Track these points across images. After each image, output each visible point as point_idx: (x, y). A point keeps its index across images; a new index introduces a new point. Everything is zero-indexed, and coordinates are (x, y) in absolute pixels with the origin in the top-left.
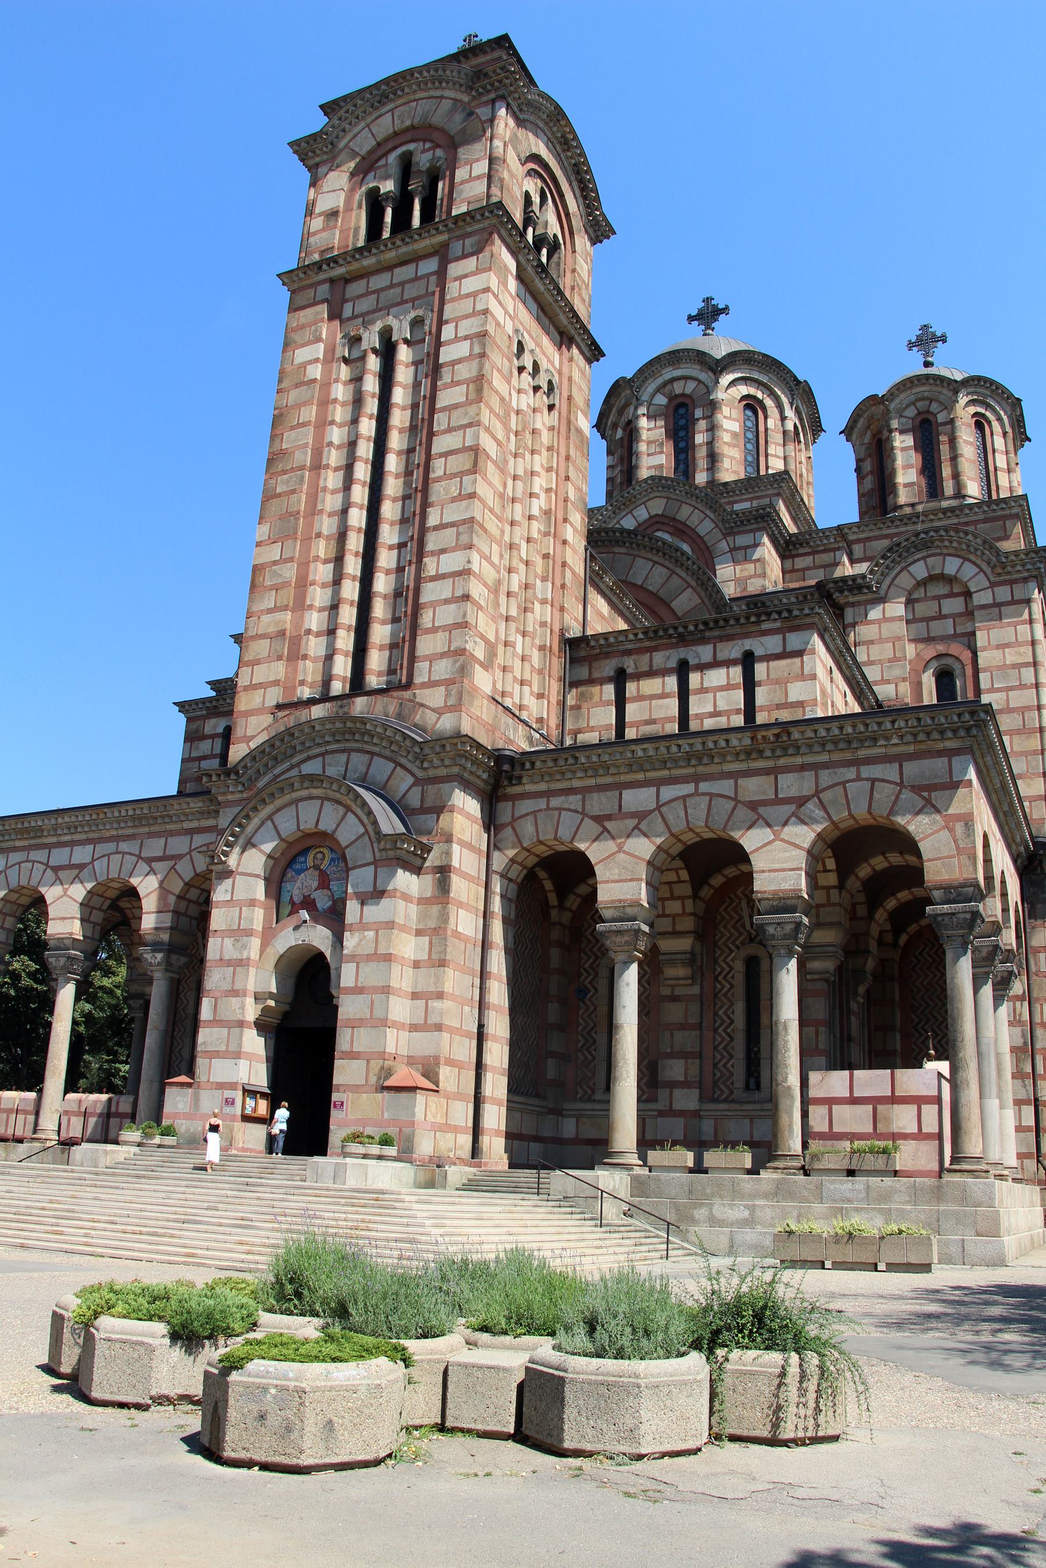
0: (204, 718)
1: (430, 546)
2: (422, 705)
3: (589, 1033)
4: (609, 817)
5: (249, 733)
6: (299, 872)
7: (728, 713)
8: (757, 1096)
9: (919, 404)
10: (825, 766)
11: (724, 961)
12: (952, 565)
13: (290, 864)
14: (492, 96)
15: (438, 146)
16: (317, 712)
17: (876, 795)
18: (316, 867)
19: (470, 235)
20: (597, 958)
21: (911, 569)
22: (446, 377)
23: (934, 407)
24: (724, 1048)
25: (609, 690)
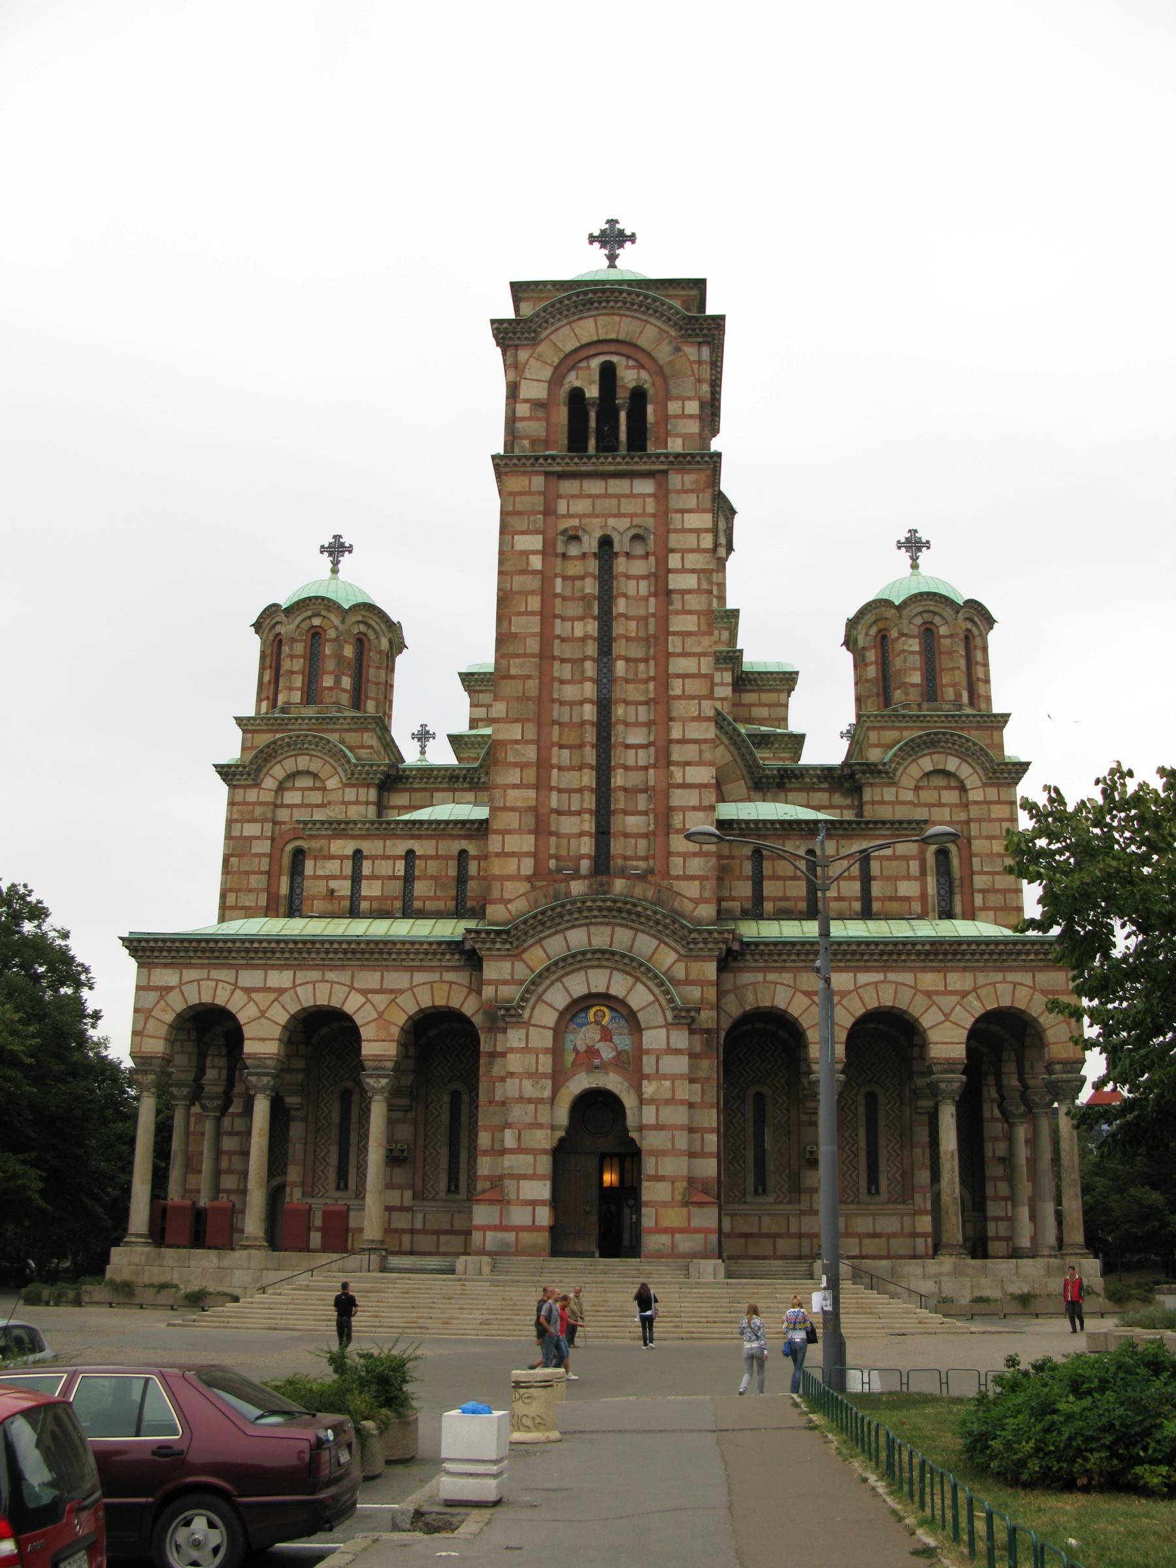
0: (330, 838)
1: (675, 757)
2: (679, 894)
5: (506, 896)
6: (581, 1025)
7: (850, 899)
8: (877, 1199)
9: (925, 615)
10: (982, 969)
12: (952, 764)
13: (571, 1020)
14: (700, 340)
15: (641, 366)
16: (577, 888)
17: (1017, 995)
18: (597, 1023)
19: (689, 471)
21: (920, 761)
22: (677, 605)
23: (937, 620)
24: (850, 1163)
25: (747, 868)
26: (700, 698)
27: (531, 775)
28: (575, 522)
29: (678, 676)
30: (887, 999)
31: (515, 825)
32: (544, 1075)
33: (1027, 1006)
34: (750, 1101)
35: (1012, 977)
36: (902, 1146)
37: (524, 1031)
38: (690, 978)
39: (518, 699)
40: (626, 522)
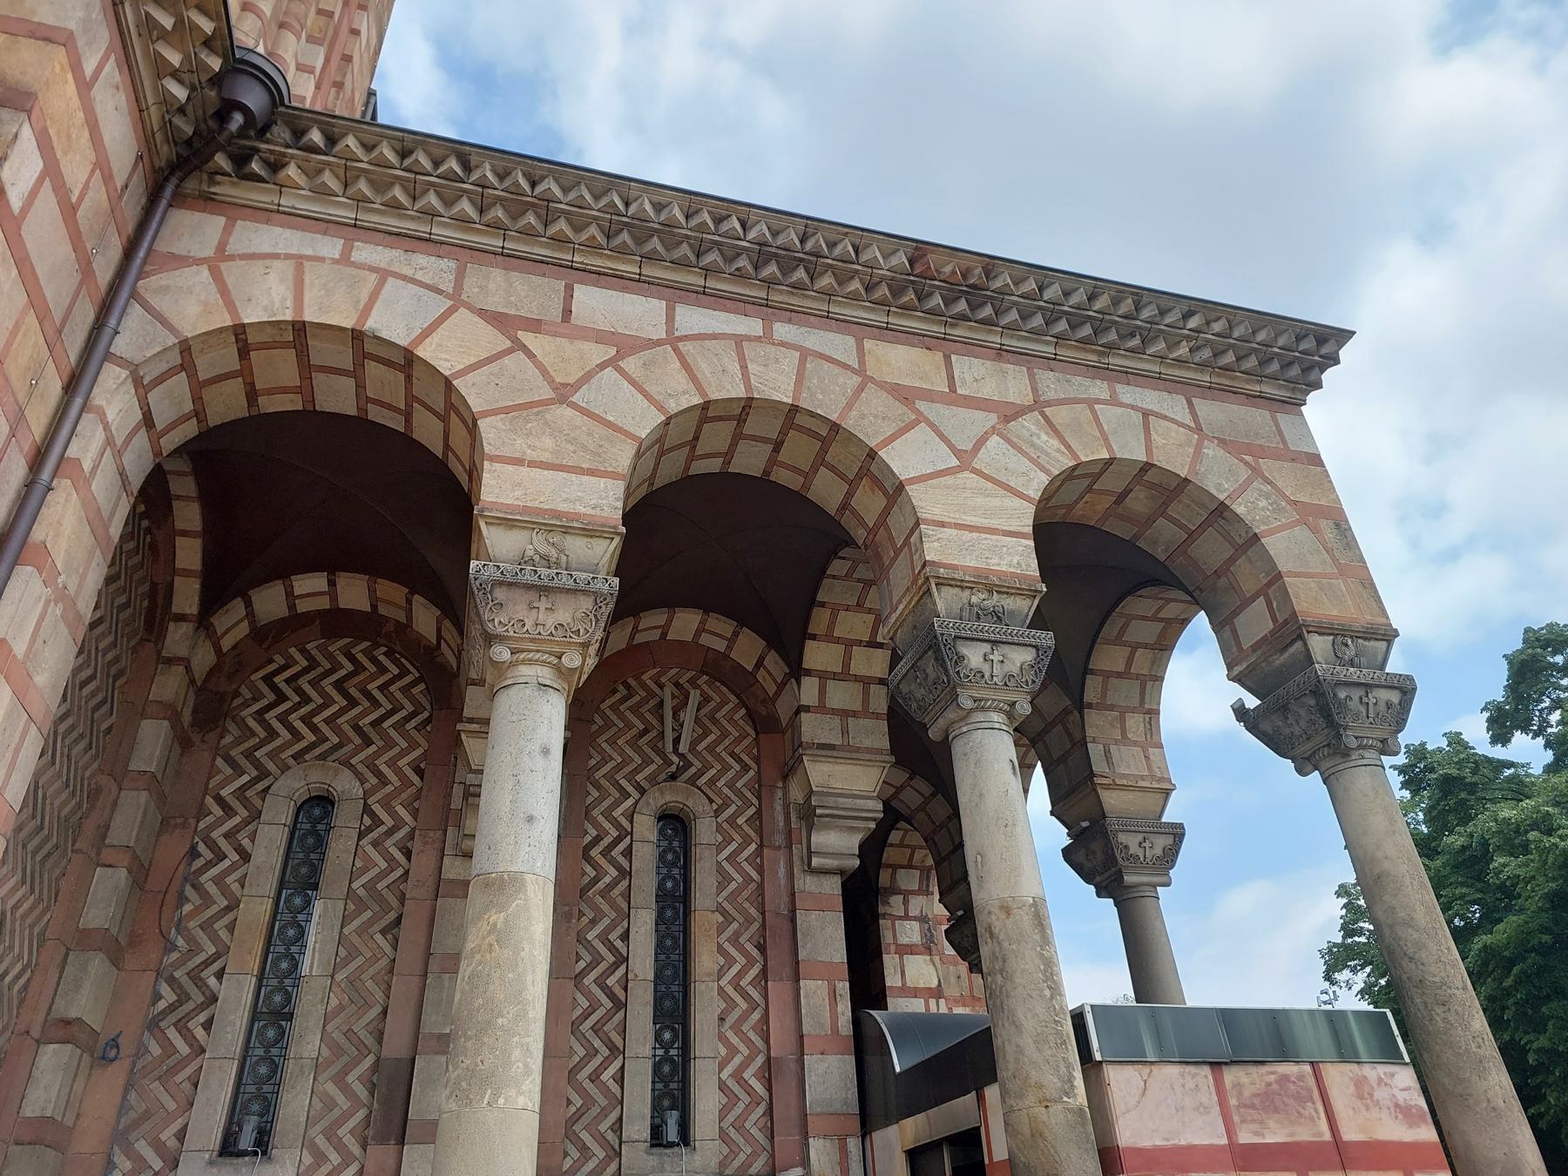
3: (195, 977)
4: (535, 326)
11: (607, 814)
20: (263, 774)
24: (595, 1029)
30: (775, 382)
34: (278, 815)
35: (1127, 394)
36: (764, 973)
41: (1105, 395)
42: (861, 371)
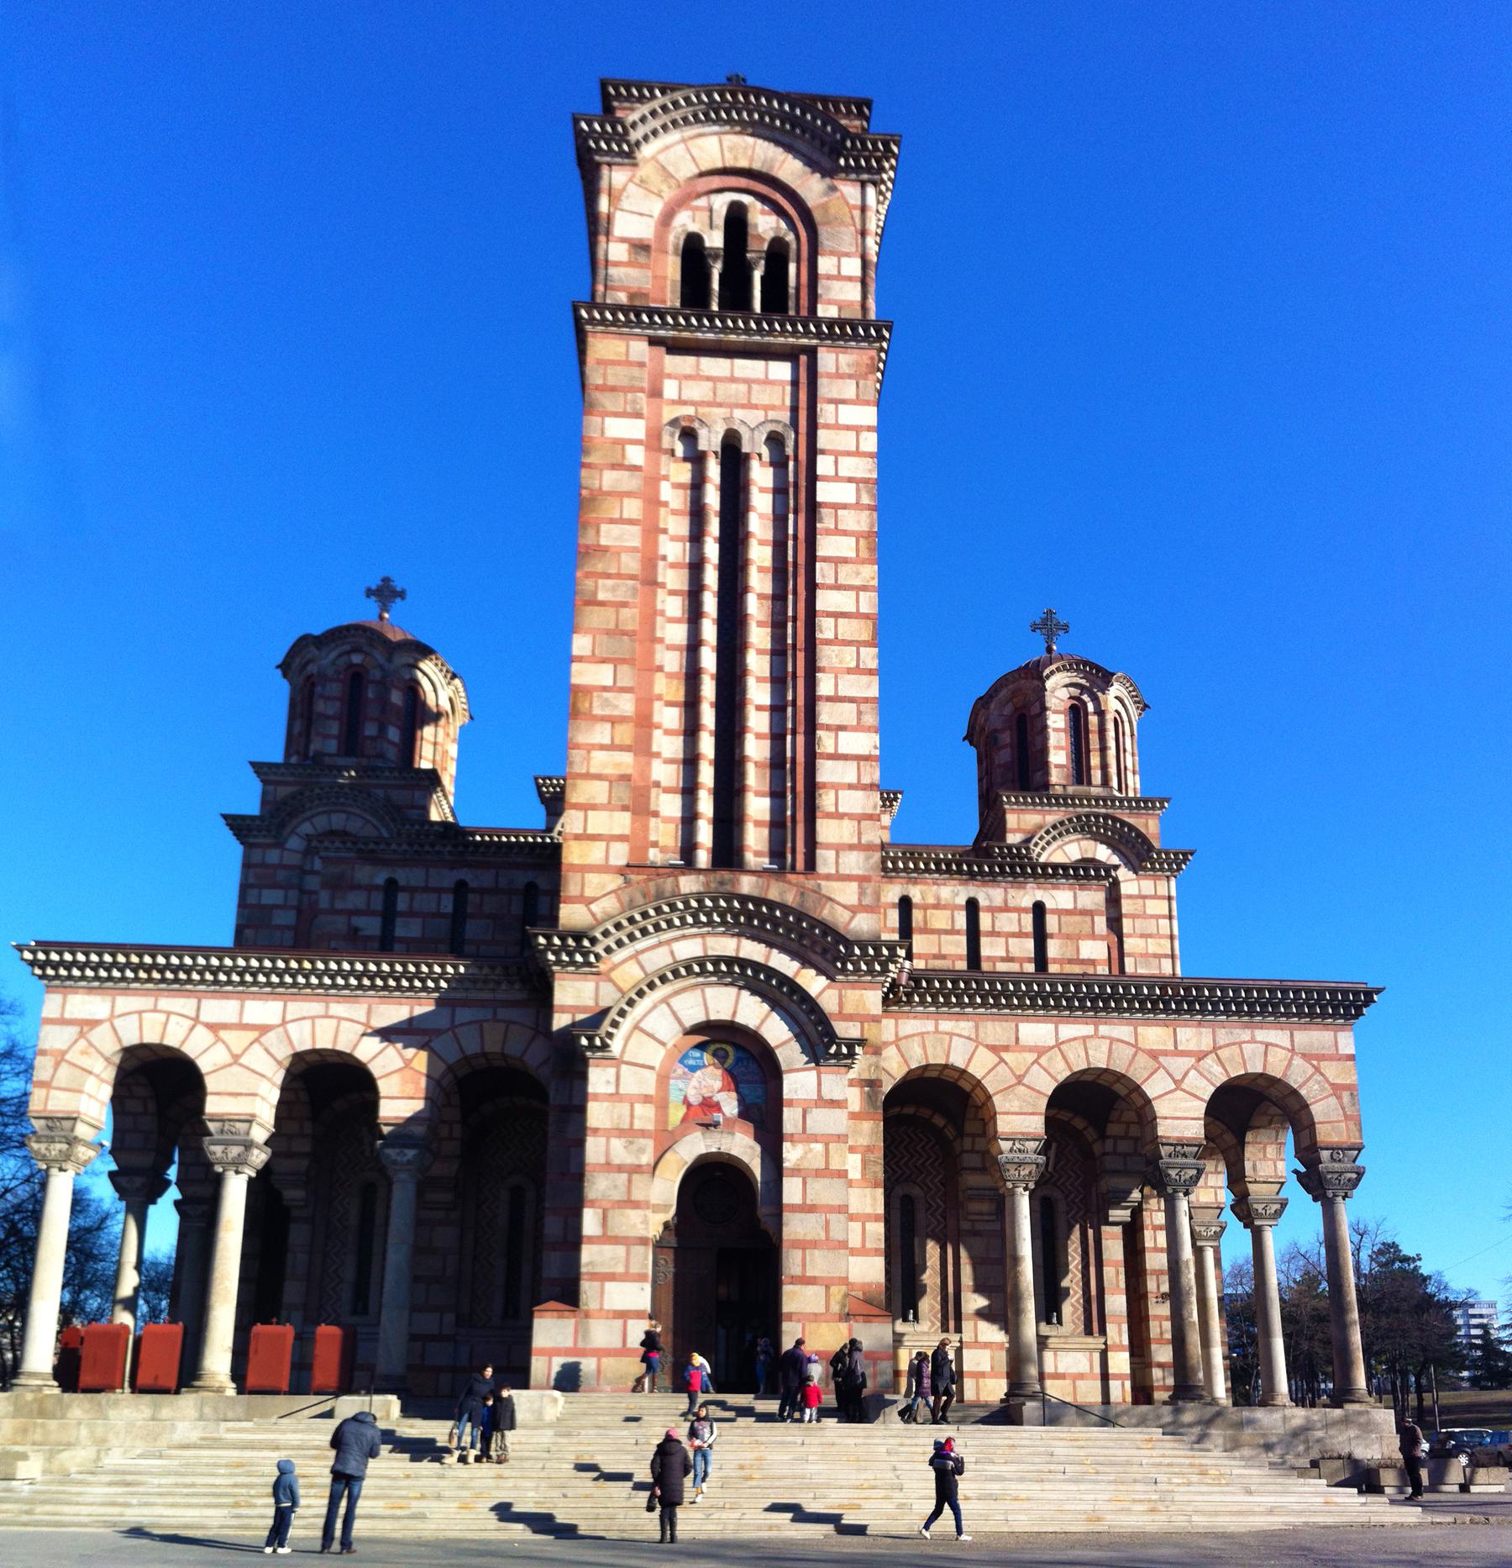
4: (1006, 1048)
5: (588, 893)
6: (693, 1069)
16: (689, 884)
17: (1270, 1059)
22: (826, 521)
26: (858, 644)
27: (625, 734)
28: (689, 411)
29: (829, 614)
31: (602, 798)
32: (643, 1133)
33: (1285, 1074)
35: (1263, 1035)
37: (612, 1071)
38: (846, 1011)
39: (608, 632)
40: (759, 415)
41: (1248, 1038)
42: (1135, 1046)
